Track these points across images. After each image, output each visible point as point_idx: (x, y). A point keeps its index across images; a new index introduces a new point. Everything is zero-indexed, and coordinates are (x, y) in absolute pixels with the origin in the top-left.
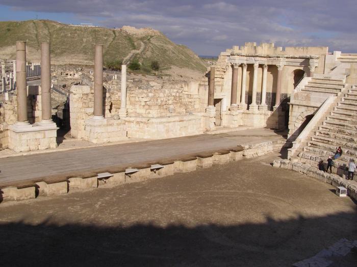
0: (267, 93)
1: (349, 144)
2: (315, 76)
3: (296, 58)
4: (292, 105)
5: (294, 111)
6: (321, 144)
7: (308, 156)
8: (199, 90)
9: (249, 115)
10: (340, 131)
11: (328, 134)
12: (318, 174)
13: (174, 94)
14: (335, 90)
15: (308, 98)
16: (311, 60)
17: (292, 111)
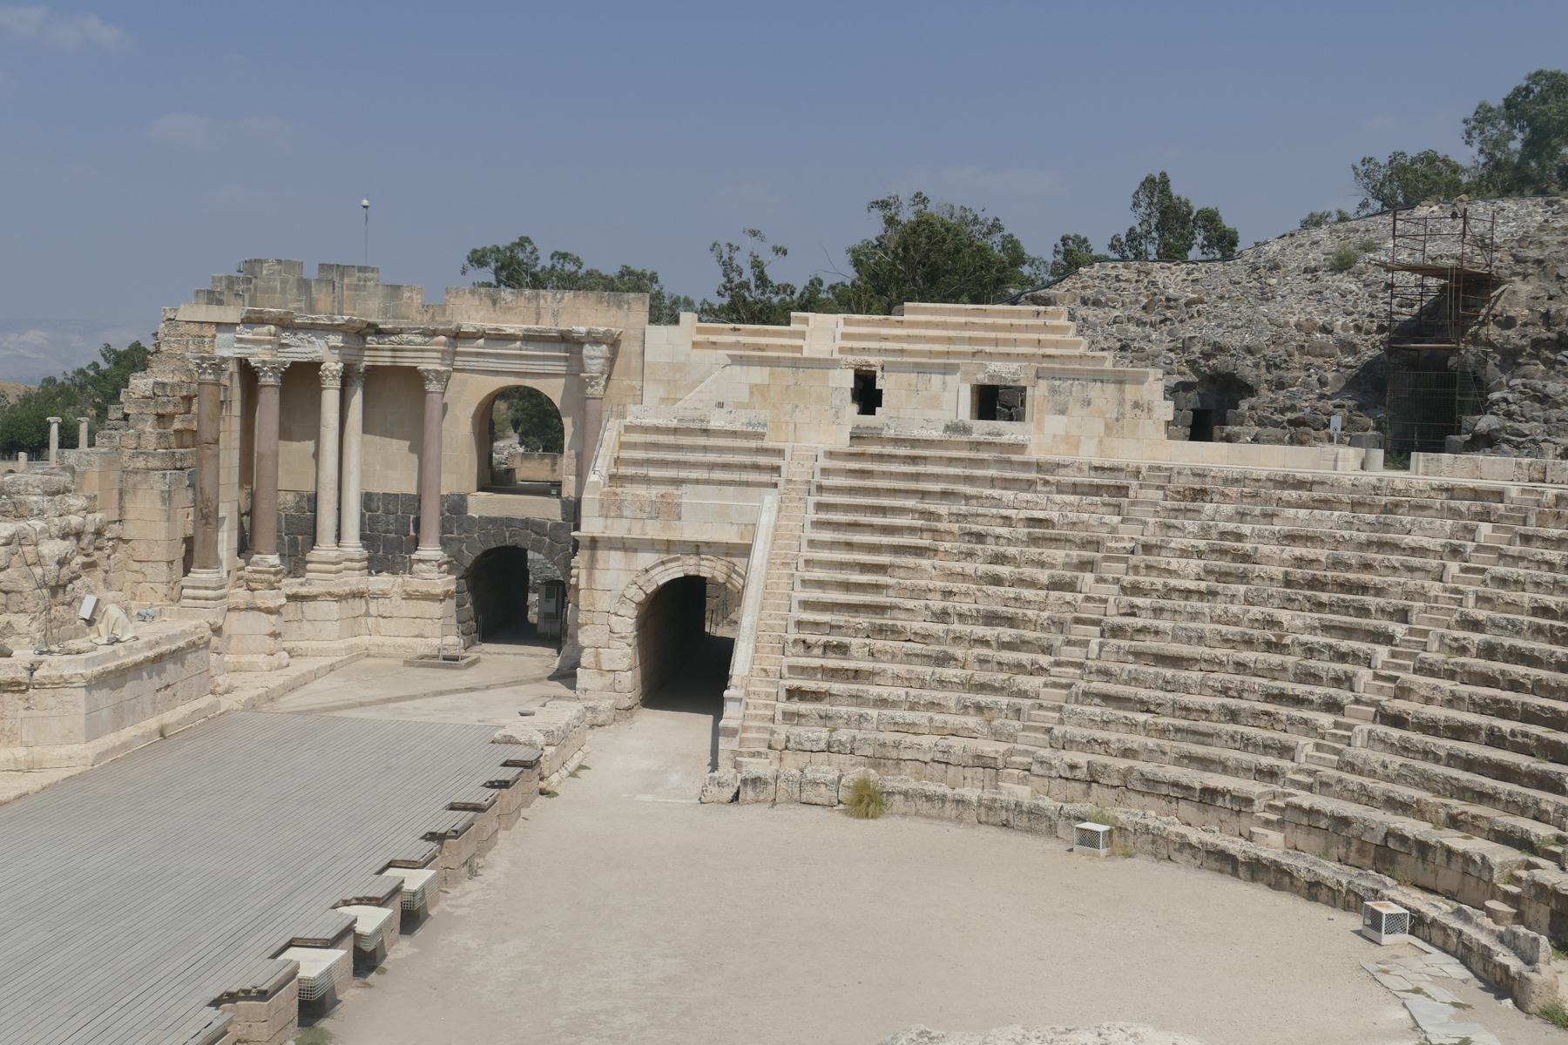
0: (367, 500)
1: (949, 673)
2: (635, 415)
3: (511, 338)
4: (594, 543)
5: (600, 564)
6: (837, 687)
7: (818, 741)
8: (121, 493)
9: (309, 607)
10: (880, 631)
11: (842, 649)
12: (929, 798)
13: (75, 520)
14: (758, 465)
15: (668, 510)
16: (588, 350)
17: (592, 566)
